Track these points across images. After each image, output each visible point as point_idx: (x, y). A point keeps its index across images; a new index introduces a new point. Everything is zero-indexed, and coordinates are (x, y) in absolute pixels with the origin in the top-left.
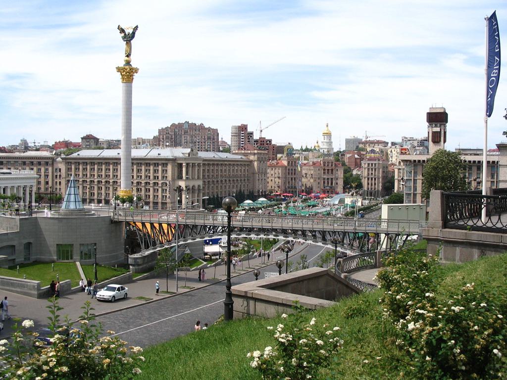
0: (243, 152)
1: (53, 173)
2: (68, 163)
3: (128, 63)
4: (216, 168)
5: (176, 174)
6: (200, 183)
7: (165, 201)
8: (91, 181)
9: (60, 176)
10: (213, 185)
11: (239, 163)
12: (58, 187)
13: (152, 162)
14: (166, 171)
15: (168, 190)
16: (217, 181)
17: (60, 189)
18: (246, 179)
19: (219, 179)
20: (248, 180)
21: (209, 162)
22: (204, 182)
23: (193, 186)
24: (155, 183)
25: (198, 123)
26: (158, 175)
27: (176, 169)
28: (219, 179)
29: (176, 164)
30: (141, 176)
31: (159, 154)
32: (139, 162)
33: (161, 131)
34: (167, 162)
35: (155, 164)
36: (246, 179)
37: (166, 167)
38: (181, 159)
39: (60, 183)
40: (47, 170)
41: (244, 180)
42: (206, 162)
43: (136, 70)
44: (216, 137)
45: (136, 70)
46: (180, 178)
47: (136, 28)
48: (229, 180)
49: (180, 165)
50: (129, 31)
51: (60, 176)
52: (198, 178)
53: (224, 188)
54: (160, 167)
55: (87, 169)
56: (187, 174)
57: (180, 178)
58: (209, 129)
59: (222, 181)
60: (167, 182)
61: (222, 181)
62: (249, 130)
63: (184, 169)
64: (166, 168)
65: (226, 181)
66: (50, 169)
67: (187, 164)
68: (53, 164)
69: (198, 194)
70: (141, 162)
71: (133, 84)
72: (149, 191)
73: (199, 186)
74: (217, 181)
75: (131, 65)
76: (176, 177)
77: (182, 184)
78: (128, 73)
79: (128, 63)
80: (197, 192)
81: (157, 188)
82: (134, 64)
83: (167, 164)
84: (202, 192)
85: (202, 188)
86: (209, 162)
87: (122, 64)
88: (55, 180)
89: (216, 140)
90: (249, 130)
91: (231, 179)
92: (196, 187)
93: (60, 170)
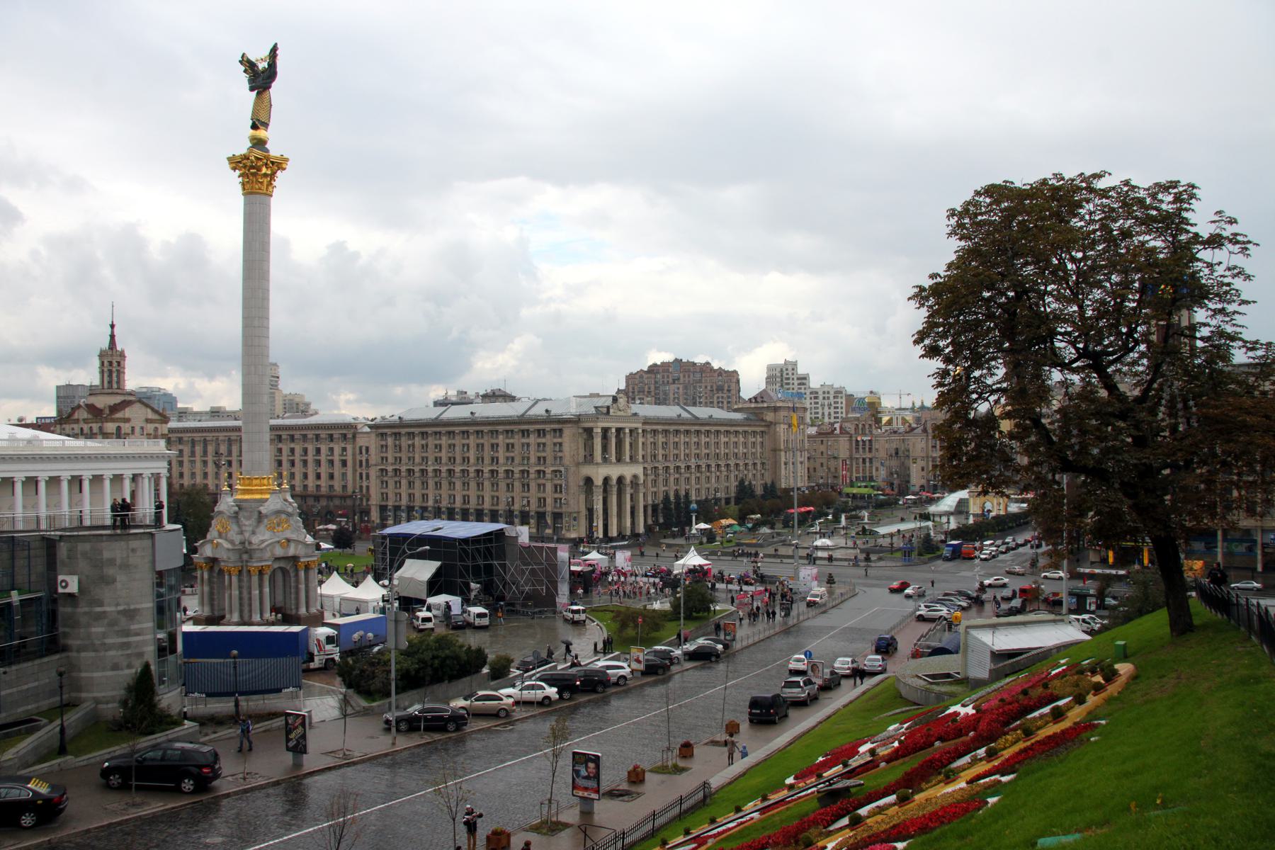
1: (354, 455)
2: (382, 434)
3: (259, 143)
5: (582, 452)
6: (638, 470)
8: (422, 471)
9: (367, 460)
12: (365, 484)
13: (531, 428)
14: (561, 444)
17: (368, 487)
18: (758, 462)
19: (693, 463)
21: (666, 427)
23: (620, 480)
24: (539, 472)
25: (700, 359)
28: (693, 463)
30: (513, 459)
31: (547, 411)
32: (508, 428)
33: (630, 378)
36: (758, 462)
37: (561, 436)
38: (588, 417)
39: (368, 477)
40: (344, 449)
41: (755, 464)
42: (648, 428)
43: (278, 165)
44: (733, 385)
45: (278, 165)
46: (589, 459)
47: (274, 50)
49: (589, 431)
50: (262, 65)
51: (367, 460)
55: (413, 445)
56: (605, 449)
57: (589, 459)
58: (721, 372)
61: (699, 467)
62: (801, 370)
64: (559, 440)
66: (349, 447)
67: (605, 431)
68: (354, 437)
71: (274, 202)
73: (635, 477)
74: (688, 467)
75: (267, 151)
76: (581, 459)
77: (599, 473)
78: (257, 171)
79: (259, 143)
82: (274, 150)
83: (561, 430)
84: (642, 490)
86: (666, 427)
87: (242, 147)
88: (359, 470)
89: (733, 392)
90: (801, 370)
91: (722, 463)
92: (628, 480)
93: (367, 449)
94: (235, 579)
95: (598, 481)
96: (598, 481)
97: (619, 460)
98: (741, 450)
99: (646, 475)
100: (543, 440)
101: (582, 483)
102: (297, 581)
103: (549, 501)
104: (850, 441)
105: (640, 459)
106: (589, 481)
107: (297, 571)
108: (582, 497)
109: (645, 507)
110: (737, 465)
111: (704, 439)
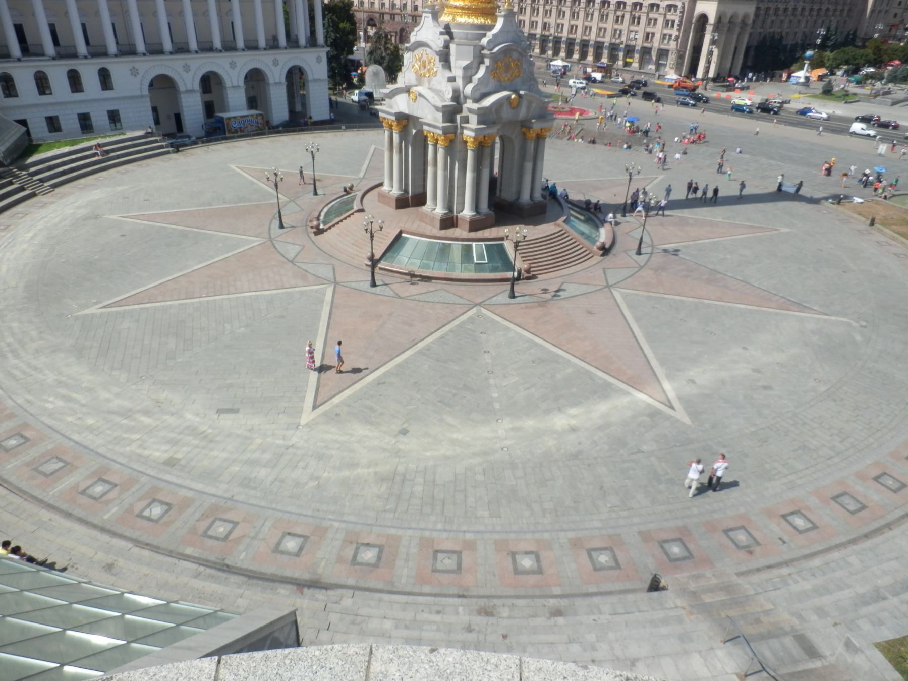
10: (774, 18)
15: (677, 22)
16: (786, 10)
20: (850, 10)
22: (758, 8)
36: (847, 8)
41: (842, 10)
48: (811, 10)
53: (803, 25)
59: (795, 9)
65: (803, 9)
69: (739, 34)
72: (638, 23)
73: (746, 16)
80: (737, 30)
81: (656, 16)
85: (750, 21)
94: (441, 153)
95: (712, 19)
96: (712, 19)
99: (757, 15)
102: (523, 158)
107: (524, 138)
109: (748, 49)
110: (828, 10)
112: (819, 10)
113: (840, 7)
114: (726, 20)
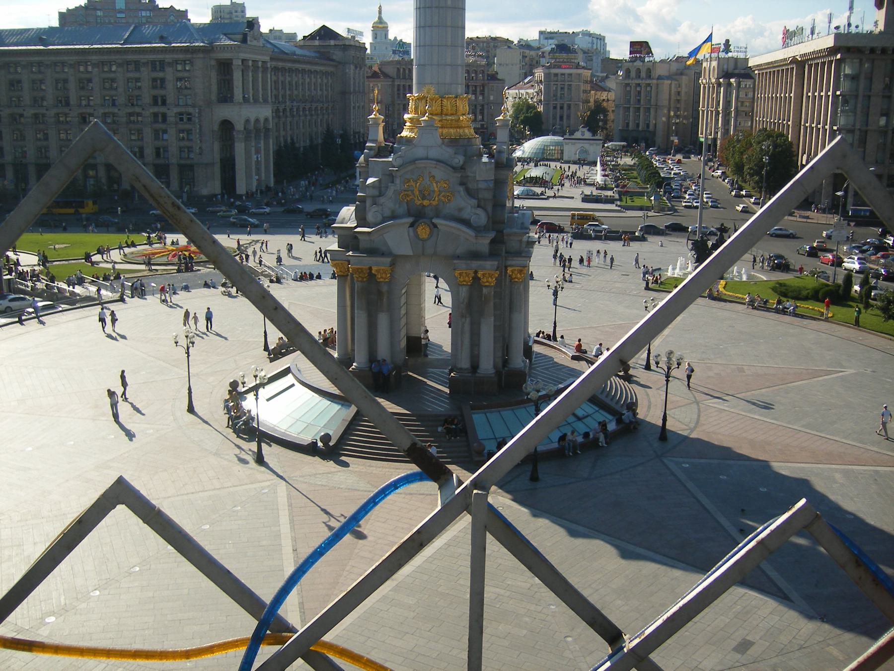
0: (317, 43)
4: (295, 79)
6: (265, 112)
7: (188, 162)
11: (318, 68)
24: (155, 115)
26: (162, 92)
27: (214, 75)
29: (213, 63)
34: (189, 56)
35: (153, 63)
52: (265, 101)
54: (169, 70)
57: (226, 97)
60: (191, 110)
63: (237, 76)
70: (113, 57)
73: (266, 120)
74: (285, 110)
76: (214, 97)
96: (239, 126)
97: (256, 101)
98: (319, 93)
100: (161, 75)
101: (216, 128)
103: (173, 150)
104: (393, 85)
105: (261, 100)
106: (227, 126)
108: (217, 146)
111: (295, 79)
112: (285, 110)
113: (326, 105)
114: (251, 126)
